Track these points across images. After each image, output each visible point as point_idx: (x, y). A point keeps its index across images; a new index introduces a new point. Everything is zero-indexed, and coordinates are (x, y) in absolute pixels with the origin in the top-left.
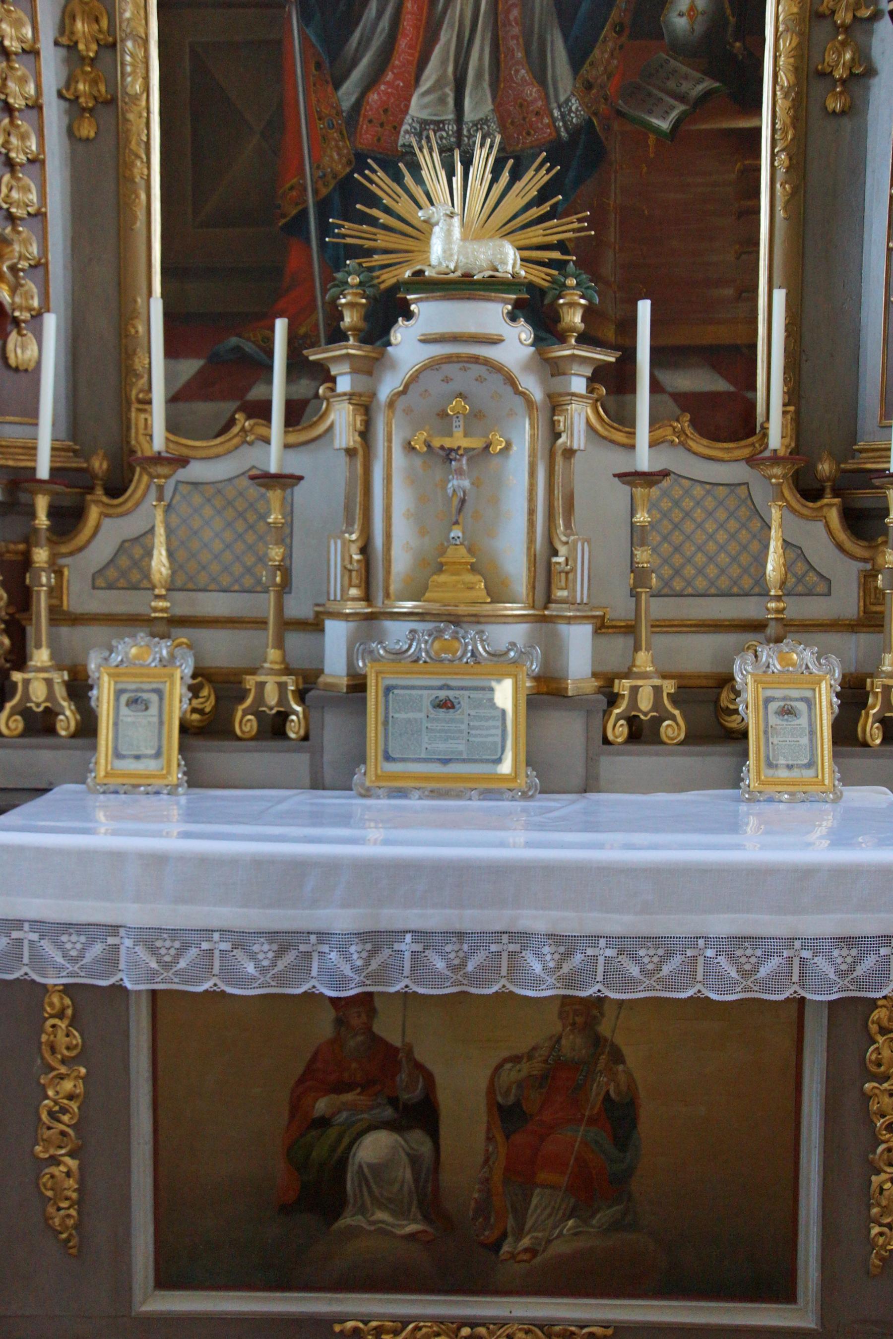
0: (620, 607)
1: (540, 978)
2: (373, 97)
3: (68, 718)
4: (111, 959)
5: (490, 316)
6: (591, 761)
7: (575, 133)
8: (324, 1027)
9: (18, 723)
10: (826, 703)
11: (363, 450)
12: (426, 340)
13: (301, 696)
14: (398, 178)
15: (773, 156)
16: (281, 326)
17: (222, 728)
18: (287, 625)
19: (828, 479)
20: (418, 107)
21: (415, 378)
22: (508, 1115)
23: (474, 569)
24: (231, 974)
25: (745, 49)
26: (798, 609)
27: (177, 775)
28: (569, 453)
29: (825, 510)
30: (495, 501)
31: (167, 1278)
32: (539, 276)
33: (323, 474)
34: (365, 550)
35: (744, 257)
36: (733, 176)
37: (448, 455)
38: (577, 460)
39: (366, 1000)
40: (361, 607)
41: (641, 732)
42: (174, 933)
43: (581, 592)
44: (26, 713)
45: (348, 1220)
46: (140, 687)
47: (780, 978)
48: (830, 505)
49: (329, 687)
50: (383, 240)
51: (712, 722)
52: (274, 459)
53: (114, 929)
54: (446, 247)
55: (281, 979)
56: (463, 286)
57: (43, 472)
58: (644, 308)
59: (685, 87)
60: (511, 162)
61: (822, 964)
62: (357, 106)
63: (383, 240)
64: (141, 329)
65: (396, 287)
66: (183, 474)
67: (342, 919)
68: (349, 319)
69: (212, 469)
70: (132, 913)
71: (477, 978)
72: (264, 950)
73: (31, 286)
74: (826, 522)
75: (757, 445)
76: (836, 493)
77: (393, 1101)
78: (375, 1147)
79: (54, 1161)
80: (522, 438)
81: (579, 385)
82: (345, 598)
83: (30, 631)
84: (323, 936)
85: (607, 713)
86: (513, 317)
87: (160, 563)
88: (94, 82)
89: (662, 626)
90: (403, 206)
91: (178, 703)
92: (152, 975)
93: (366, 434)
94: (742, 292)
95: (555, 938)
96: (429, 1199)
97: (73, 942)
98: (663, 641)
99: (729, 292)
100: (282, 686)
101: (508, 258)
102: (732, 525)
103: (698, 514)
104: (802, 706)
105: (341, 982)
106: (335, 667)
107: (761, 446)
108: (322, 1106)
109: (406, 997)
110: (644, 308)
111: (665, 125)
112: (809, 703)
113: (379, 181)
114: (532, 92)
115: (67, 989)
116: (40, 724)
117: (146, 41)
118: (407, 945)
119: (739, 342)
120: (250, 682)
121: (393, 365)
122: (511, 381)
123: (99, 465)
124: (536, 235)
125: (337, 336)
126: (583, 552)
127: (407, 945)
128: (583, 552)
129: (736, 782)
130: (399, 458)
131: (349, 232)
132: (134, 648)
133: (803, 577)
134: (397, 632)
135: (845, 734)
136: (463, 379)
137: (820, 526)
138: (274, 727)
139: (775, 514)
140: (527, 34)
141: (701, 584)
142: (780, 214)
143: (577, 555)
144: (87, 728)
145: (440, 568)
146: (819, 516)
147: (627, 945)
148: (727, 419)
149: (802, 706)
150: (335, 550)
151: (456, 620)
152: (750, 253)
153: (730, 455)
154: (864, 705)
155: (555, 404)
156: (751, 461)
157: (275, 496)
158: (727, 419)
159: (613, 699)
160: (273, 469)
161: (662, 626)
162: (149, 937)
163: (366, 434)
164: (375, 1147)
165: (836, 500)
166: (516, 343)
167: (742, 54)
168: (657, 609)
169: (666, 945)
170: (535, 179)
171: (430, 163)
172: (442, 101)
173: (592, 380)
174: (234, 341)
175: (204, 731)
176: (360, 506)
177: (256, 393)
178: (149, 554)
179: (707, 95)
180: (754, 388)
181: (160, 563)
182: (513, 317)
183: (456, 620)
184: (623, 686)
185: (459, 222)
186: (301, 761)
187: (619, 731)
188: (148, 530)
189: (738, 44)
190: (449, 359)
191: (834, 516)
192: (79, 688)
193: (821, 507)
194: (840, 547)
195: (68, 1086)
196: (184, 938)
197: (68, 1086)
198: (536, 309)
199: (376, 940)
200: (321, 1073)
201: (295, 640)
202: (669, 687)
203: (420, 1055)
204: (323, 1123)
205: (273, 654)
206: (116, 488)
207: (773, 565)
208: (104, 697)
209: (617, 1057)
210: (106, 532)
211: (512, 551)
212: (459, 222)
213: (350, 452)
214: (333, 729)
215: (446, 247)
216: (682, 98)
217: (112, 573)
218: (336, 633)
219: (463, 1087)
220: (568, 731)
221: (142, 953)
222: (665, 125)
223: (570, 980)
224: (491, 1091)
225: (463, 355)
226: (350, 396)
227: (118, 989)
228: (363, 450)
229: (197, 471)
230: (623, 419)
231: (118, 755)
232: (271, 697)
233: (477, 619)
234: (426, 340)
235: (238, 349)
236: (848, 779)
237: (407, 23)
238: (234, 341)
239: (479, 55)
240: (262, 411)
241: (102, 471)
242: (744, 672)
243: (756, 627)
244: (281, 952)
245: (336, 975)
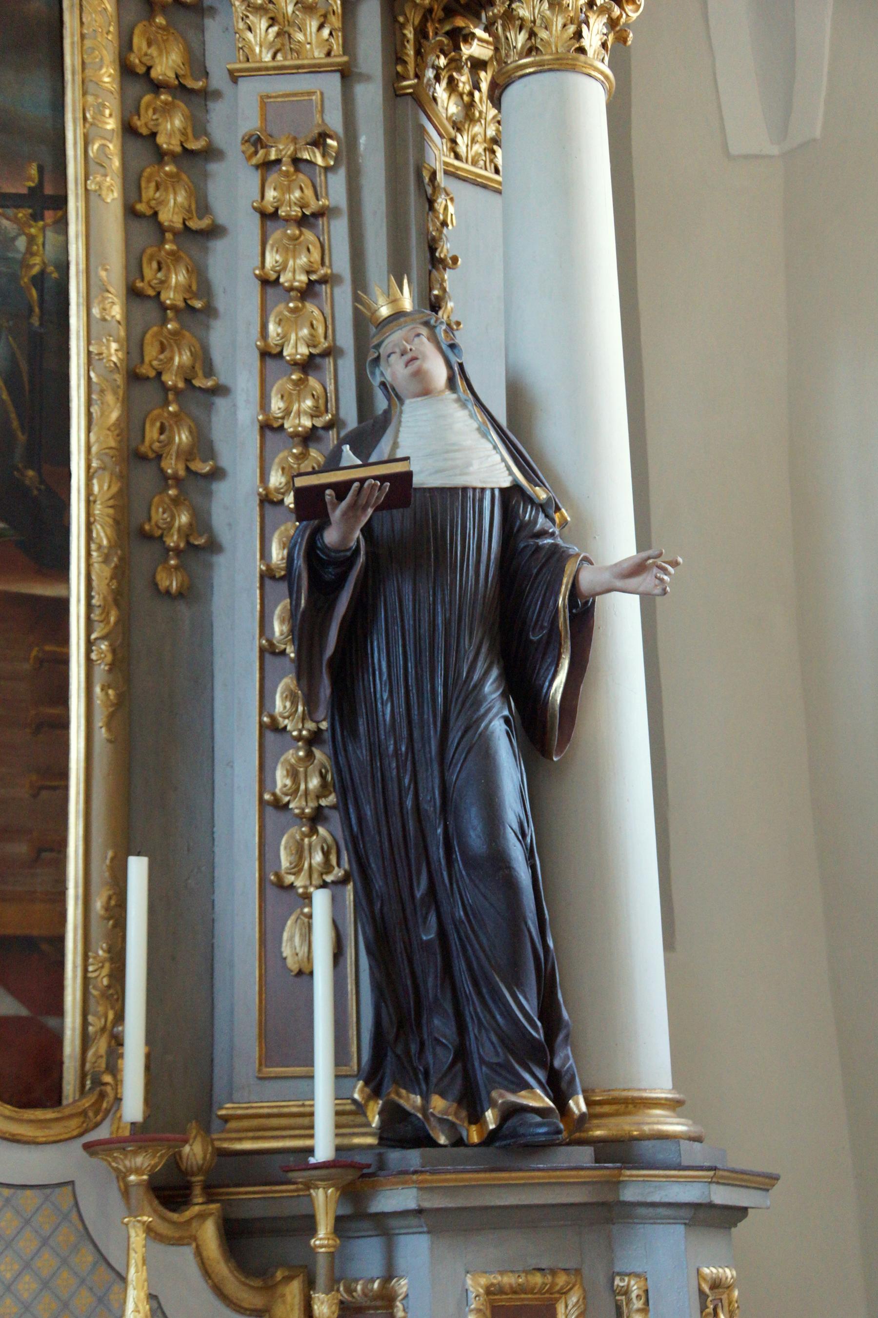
15: (89, 645)
19: (200, 1169)
25: (42, 482)
29: (194, 1224)
35: (44, 794)
36: (27, 666)
48: (202, 1217)
74: (198, 1247)
75: (91, 1114)
76: (211, 1192)
94: (40, 851)
99: (21, 849)
102: (46, 1262)
107: (96, 1114)
119: (35, 932)
137: (188, 1252)
142: (101, 733)
146: (185, 1237)
152: (55, 788)
153: (47, 1132)
165: (214, 1207)
167: (39, 490)
180: (59, 1010)
189: (31, 473)
191: (209, 1234)
193: (189, 1222)
194: (219, 1291)
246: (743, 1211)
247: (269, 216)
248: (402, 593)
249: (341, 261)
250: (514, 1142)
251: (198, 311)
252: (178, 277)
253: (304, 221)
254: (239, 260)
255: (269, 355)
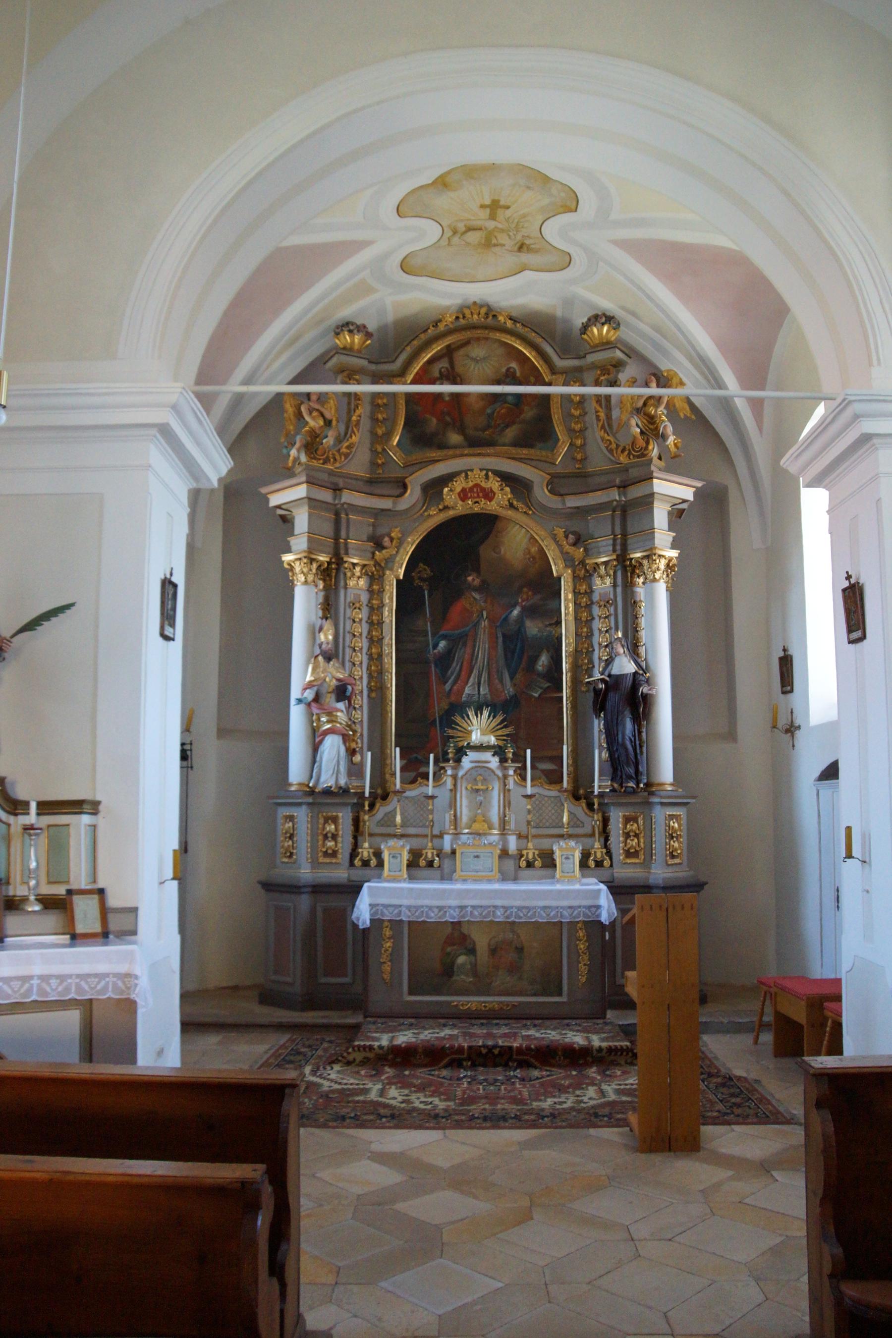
0: (524, 830)
1: (500, 916)
2: (455, 687)
3: (374, 862)
4: (400, 913)
5: (488, 756)
6: (516, 871)
7: (512, 697)
8: (449, 930)
9: (360, 863)
10: (577, 856)
11: (454, 790)
12: (472, 762)
13: (438, 856)
14: (463, 718)
16: (432, 756)
17: (416, 864)
18: (434, 836)
20: (467, 690)
21: (469, 771)
22: (493, 951)
23: (484, 821)
24: (428, 916)
26: (571, 831)
27: (406, 876)
28: (509, 790)
30: (490, 802)
31: (411, 993)
32: (501, 743)
33: (443, 794)
34: (455, 816)
37: (477, 791)
38: (511, 793)
39: (459, 923)
40: (454, 831)
41: (530, 865)
42: (415, 907)
43: (513, 826)
44: (362, 860)
45: (454, 978)
46: (395, 854)
47: (555, 916)
49: (446, 853)
50: (460, 734)
51: (548, 861)
52: (430, 791)
53: (401, 906)
54: (476, 737)
55: (440, 918)
56: (480, 748)
57: (367, 794)
58: (529, 752)
59: (542, 685)
60: (493, 714)
61: (565, 913)
62: (450, 690)
63: (460, 734)
64: (389, 752)
65: (463, 747)
66: (405, 795)
67: (454, 903)
68: (451, 755)
69: (413, 792)
70: (405, 902)
71: (485, 917)
72: (436, 910)
73: (359, 741)
77: (466, 948)
78: (461, 959)
79: (384, 963)
80: (496, 787)
81: (511, 772)
82: (450, 829)
83: (360, 838)
84: (450, 907)
85: (520, 859)
86: (494, 755)
87: (398, 819)
88: (376, 683)
89: (535, 836)
90: (465, 725)
91: (405, 856)
92: (409, 917)
93: (455, 785)
95: (503, 907)
96: (475, 973)
97: (391, 909)
98: (536, 841)
99: (556, 741)
100: (432, 853)
101: (493, 740)
103: (547, 805)
104: (571, 857)
105: (454, 918)
106: (447, 847)
108: (449, 949)
109: (468, 921)
110: (529, 752)
111: (536, 695)
112: (573, 856)
113: (458, 719)
114: (499, 686)
115: (389, 921)
116: (366, 863)
117: (391, 673)
118: (469, 909)
120: (424, 852)
121: (462, 768)
122: (493, 771)
123: (379, 791)
124: (499, 733)
125: (448, 760)
126: (513, 817)
127: (469, 909)
128: (513, 817)
129: (553, 877)
130: (464, 792)
131: (450, 732)
132: (392, 842)
133: (575, 821)
134: (464, 838)
135: (584, 864)
136: (481, 771)
138: (430, 864)
139: (566, 805)
140: (498, 671)
141: (547, 824)
143: (512, 818)
144: (380, 864)
145: (475, 821)
147: (520, 908)
148: (554, 778)
149: (571, 857)
150: (447, 816)
151: (479, 834)
154: (590, 857)
155: (505, 777)
156: (559, 791)
157: (430, 802)
158: (554, 778)
159: (522, 856)
160: (430, 794)
161: (535, 836)
162: (409, 908)
163: (455, 785)
164: (461, 959)
166: (494, 762)
168: (534, 831)
169: (528, 908)
170: (499, 718)
171: (471, 713)
172: (474, 688)
173: (515, 771)
174: (415, 755)
175: (412, 864)
176: (453, 804)
177: (423, 770)
178: (395, 818)
179: (548, 687)
181: (398, 819)
182: (494, 755)
183: (479, 834)
184: (524, 852)
185: (479, 729)
186: (438, 873)
187: (523, 864)
188: (396, 811)
190: (477, 767)
191: (584, 805)
192: (378, 854)
195: (388, 945)
196: (417, 908)
197: (388, 945)
198: (499, 751)
199: (462, 908)
200: (449, 941)
201: (436, 841)
202: (537, 852)
203: (472, 936)
204: (449, 954)
205: (430, 844)
206: (385, 797)
207: (565, 819)
208: (386, 856)
209: (519, 936)
210: (382, 810)
211: (494, 815)
212: (479, 729)
213: (451, 790)
214: (447, 863)
215: (476, 737)
216: (541, 688)
217: (382, 822)
218: (447, 839)
219: (482, 942)
220: (510, 864)
221: (407, 911)
222: (536, 695)
223: (507, 917)
224: (489, 945)
225: (480, 766)
226: (451, 776)
227: (401, 921)
228: (454, 790)
229: (408, 794)
230: (524, 778)
231: (390, 871)
232: (430, 855)
233: (485, 834)
234: (472, 762)
235: (416, 758)
236: (583, 876)
237: (464, 668)
238: (415, 755)
239: (485, 676)
240: (426, 776)
241: (382, 794)
242: (555, 848)
243: (561, 836)
244: (440, 911)
245: (452, 916)
246: (688, 803)
247: (600, 617)
248: (611, 695)
249: (613, 625)
250: (634, 792)
251: (590, 635)
252: (585, 630)
253: (606, 617)
254: (597, 625)
255: (600, 644)
